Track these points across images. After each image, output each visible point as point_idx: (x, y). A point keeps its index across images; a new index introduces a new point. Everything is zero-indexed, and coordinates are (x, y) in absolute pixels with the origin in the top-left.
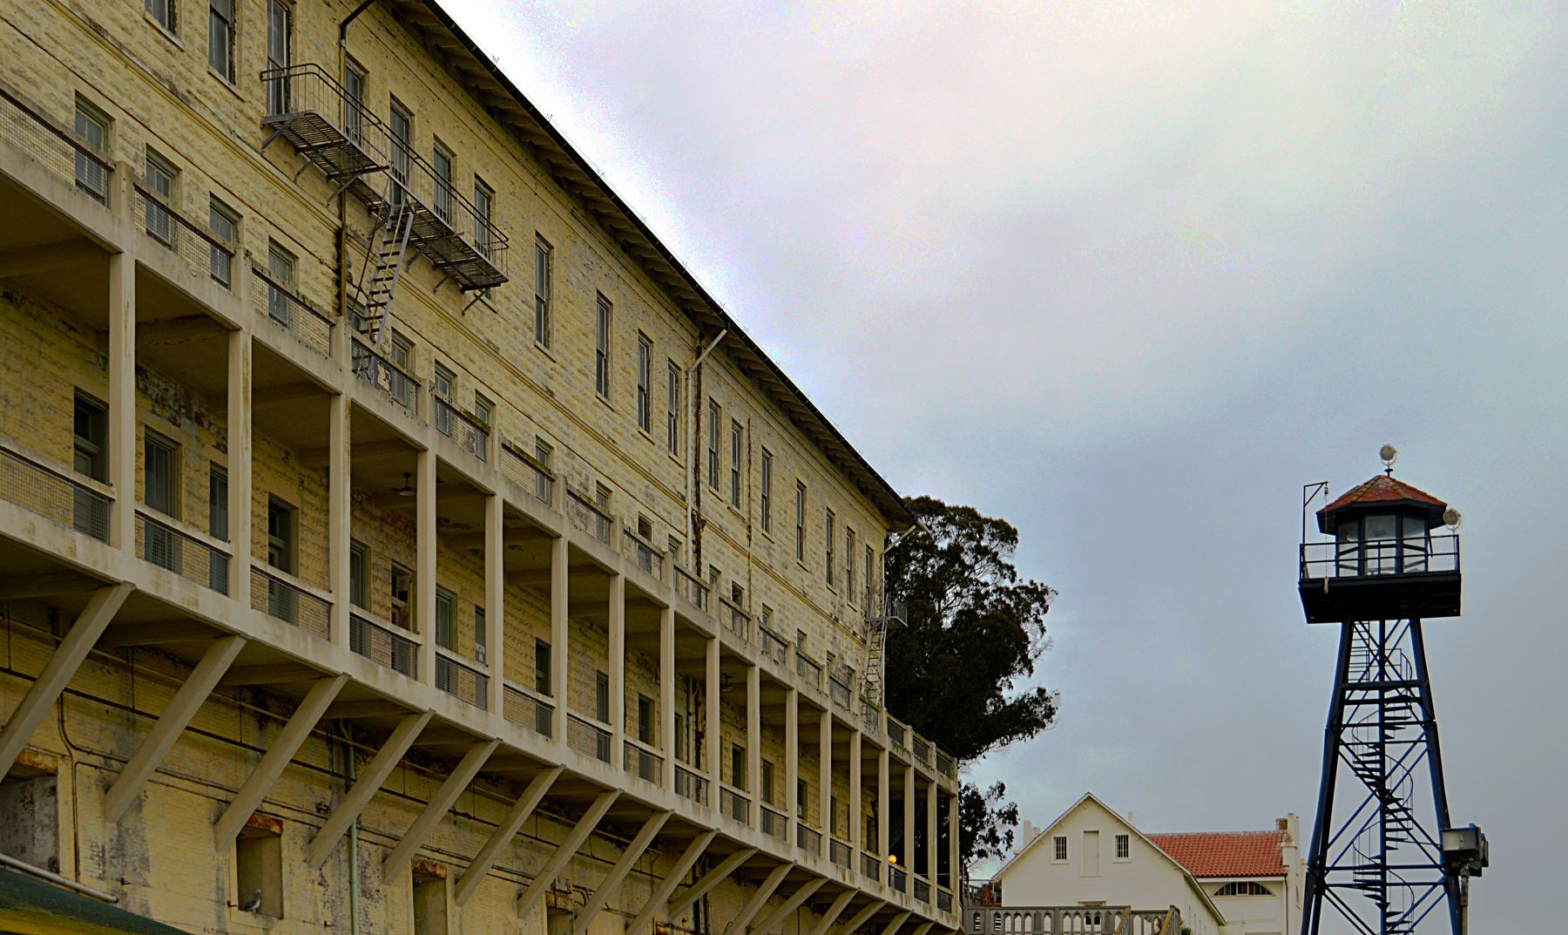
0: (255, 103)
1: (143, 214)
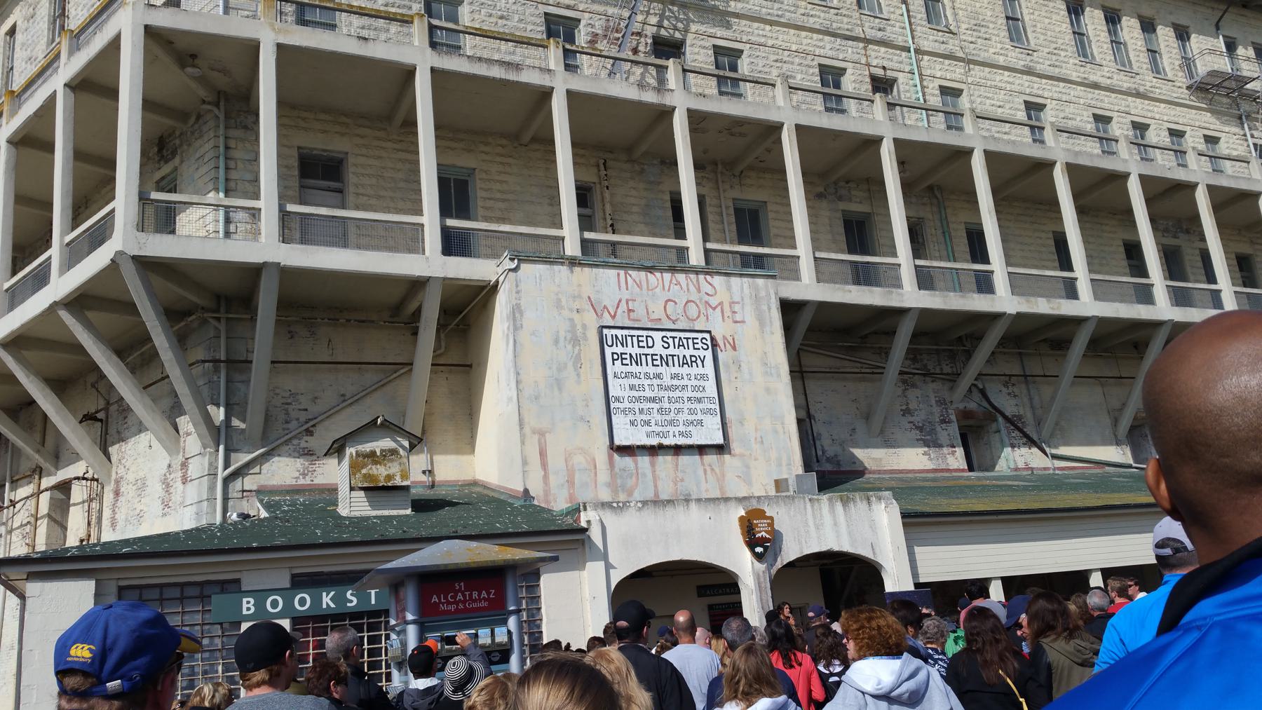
0: (1180, 79)
1: (1137, 151)
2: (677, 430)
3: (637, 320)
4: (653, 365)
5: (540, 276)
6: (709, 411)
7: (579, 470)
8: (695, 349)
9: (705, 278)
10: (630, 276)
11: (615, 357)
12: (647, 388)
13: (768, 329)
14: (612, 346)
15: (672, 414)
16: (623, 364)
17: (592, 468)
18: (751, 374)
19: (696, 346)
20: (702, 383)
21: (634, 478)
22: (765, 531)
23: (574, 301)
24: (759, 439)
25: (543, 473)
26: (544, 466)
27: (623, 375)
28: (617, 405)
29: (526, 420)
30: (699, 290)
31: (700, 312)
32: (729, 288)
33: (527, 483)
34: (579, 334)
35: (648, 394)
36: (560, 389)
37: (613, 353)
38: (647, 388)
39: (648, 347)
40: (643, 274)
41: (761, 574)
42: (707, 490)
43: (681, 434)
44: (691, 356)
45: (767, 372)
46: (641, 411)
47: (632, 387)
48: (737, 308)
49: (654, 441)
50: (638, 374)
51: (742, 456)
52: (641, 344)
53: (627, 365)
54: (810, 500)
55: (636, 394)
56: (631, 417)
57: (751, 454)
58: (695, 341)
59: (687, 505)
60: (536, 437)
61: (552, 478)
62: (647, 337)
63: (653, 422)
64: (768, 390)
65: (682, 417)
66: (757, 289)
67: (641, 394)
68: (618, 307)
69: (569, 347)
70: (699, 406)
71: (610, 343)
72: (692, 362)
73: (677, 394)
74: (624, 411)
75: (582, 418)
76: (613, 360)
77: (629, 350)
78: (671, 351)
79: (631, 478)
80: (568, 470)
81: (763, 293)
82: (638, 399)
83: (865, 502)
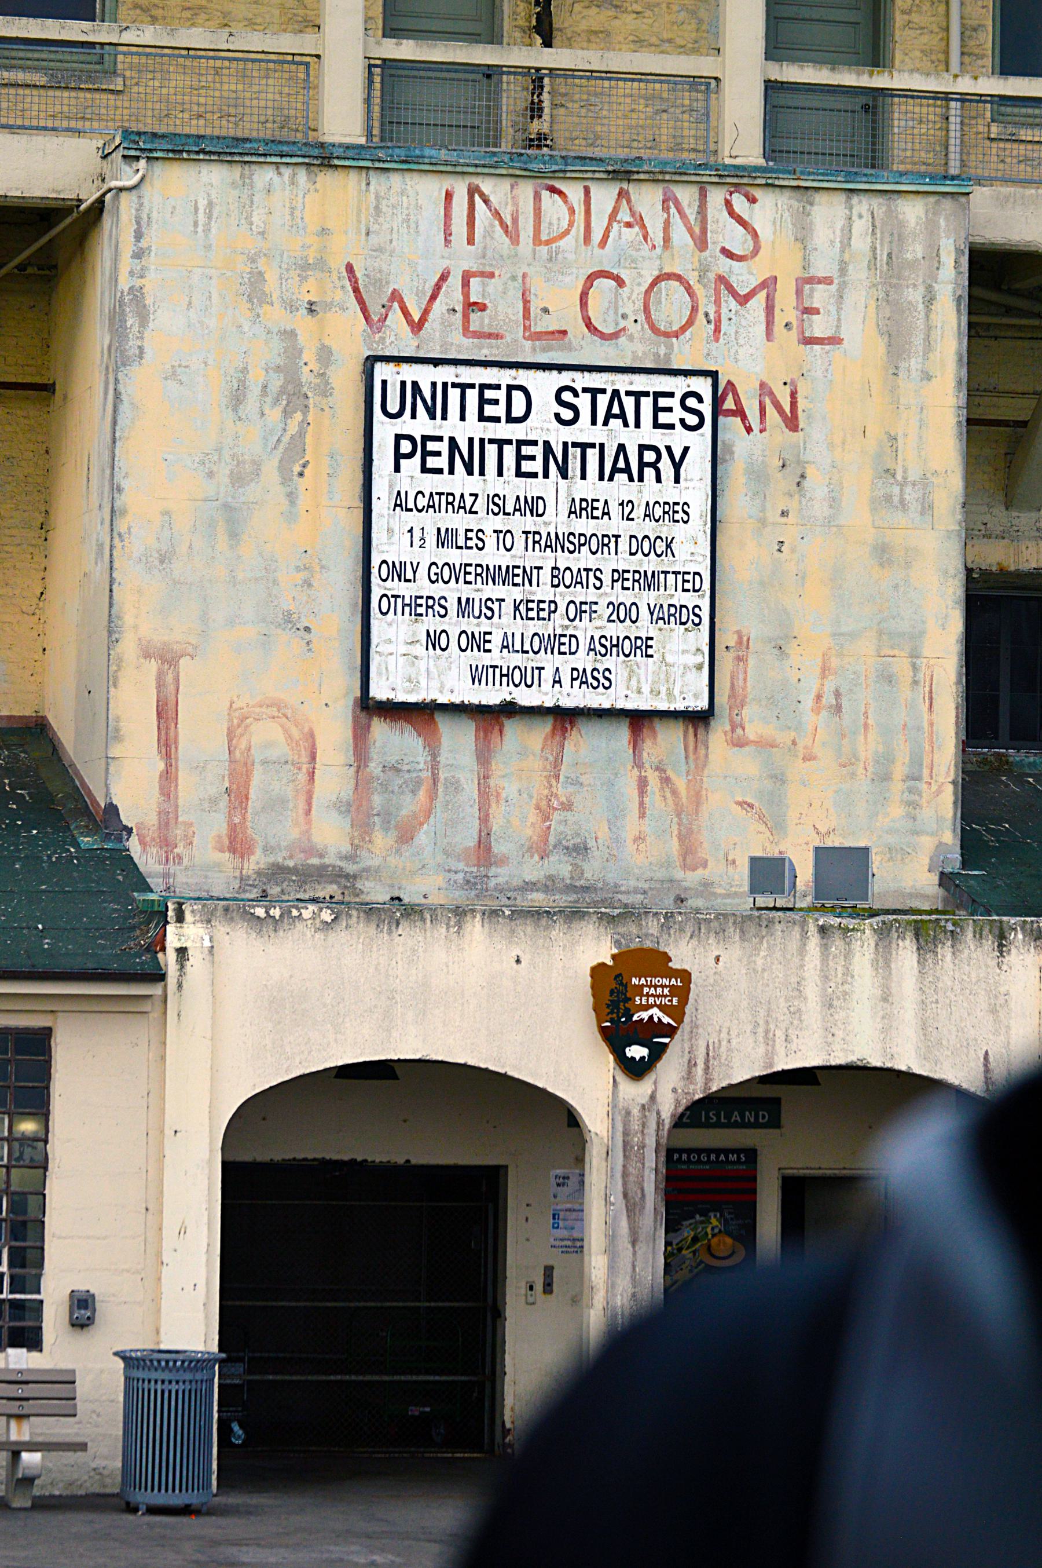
2: (566, 664)
3: (490, 336)
4: (519, 474)
5: (210, 204)
6: (676, 615)
7: (265, 762)
8: (657, 425)
9: (728, 204)
10: (486, 201)
11: (406, 447)
12: (491, 541)
13: (915, 364)
14: (400, 414)
15: (559, 619)
16: (424, 470)
17: (305, 759)
18: (834, 502)
19: (664, 418)
20: (666, 529)
21: (422, 794)
22: (661, 1008)
23: (303, 279)
24: (829, 699)
25: (161, 766)
26: (167, 745)
27: (422, 502)
28: (396, 587)
29: (128, 620)
30: (702, 243)
31: (694, 309)
32: (803, 237)
33: (112, 791)
34: (305, 375)
35: (493, 556)
36: (234, 535)
37: (399, 438)
38: (491, 541)
39: (510, 419)
40: (526, 190)
41: (636, 1112)
42: (639, 839)
43: (579, 677)
44: (642, 448)
45: (888, 498)
46: (465, 607)
47: (445, 538)
48: (819, 296)
49: (492, 695)
50: (469, 500)
51: (766, 744)
52: (489, 410)
53: (440, 471)
54: (823, 930)
55: (455, 557)
56: (432, 623)
57: (794, 743)
58: (663, 402)
59: (460, 925)
60: (153, 666)
61: (185, 779)
62: (510, 388)
63: (496, 639)
64: (883, 553)
65: (585, 629)
66: (898, 236)
67: (472, 556)
68: (433, 297)
69: (275, 415)
70: (647, 598)
71: (393, 407)
72: (642, 465)
73: (584, 559)
74: (414, 607)
75: (288, 619)
76: (398, 456)
77: (452, 427)
78: (583, 431)
79: (413, 792)
80: (232, 761)
81: (915, 250)
82: (460, 573)
83: (989, 943)
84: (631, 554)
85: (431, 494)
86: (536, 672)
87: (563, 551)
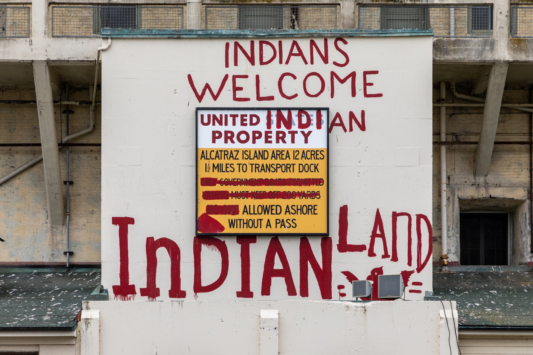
27: (213, 155)
84: (300, 172)
85: (217, 151)
86: (259, 221)
87: (270, 172)
